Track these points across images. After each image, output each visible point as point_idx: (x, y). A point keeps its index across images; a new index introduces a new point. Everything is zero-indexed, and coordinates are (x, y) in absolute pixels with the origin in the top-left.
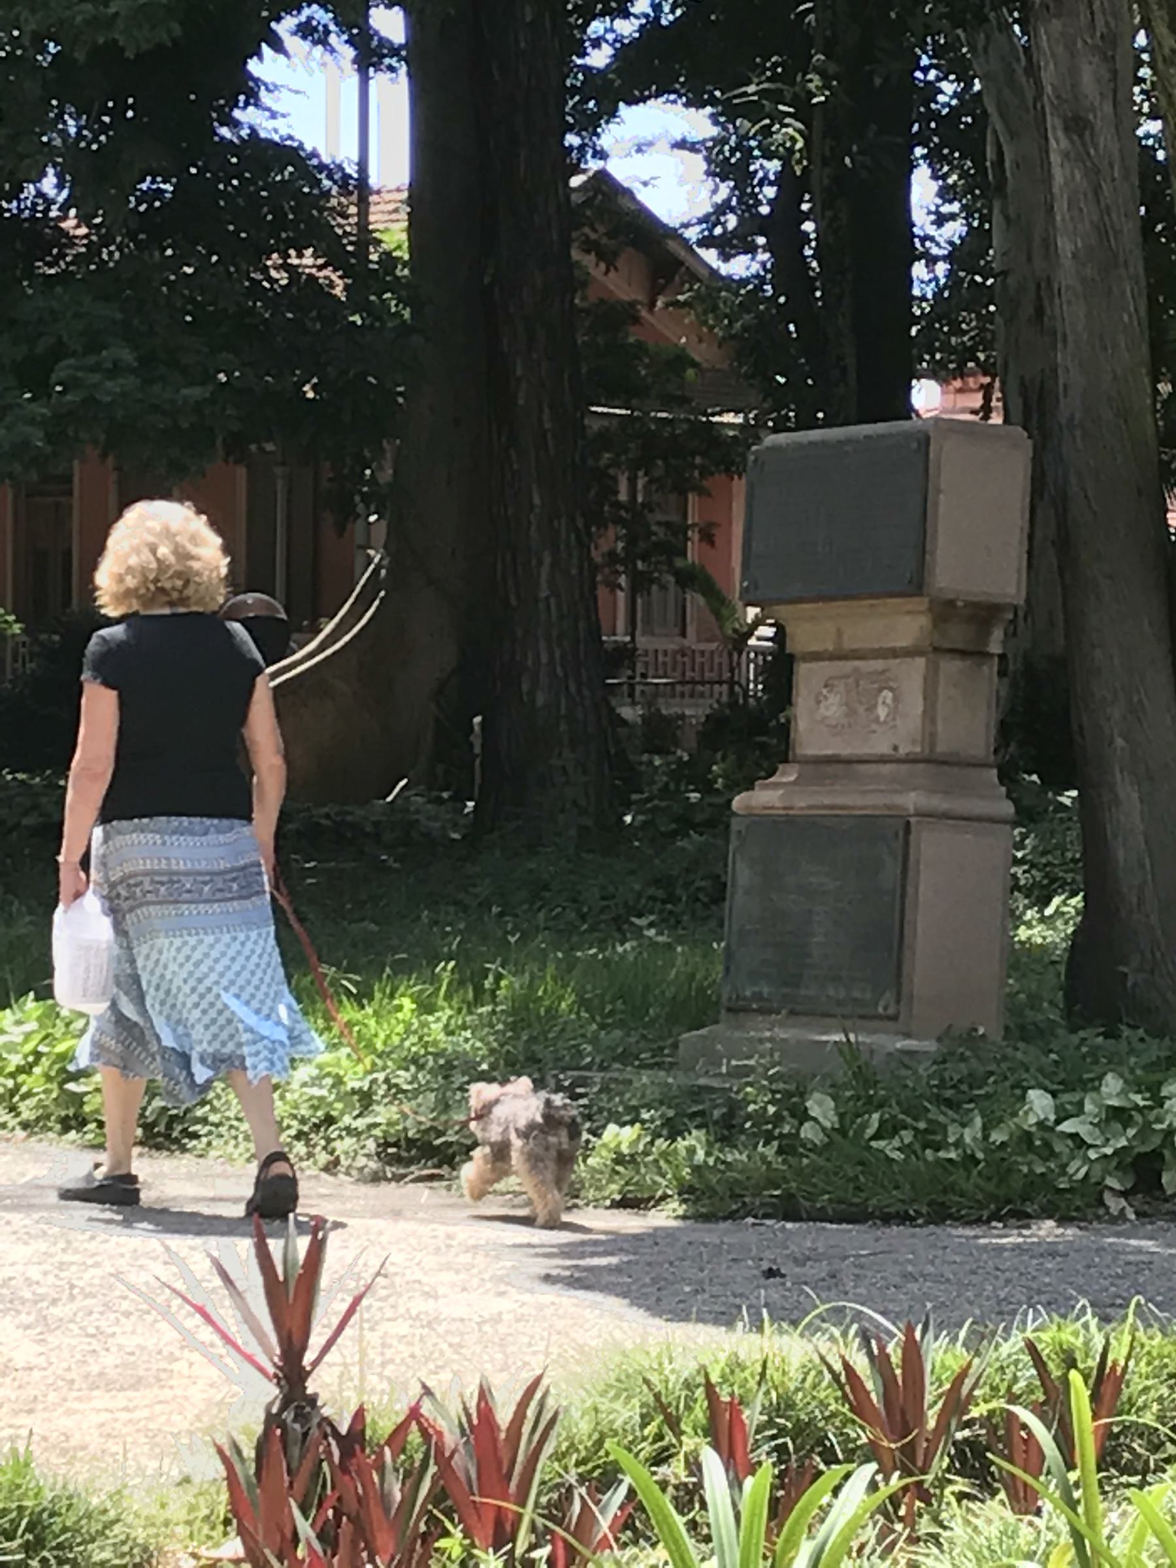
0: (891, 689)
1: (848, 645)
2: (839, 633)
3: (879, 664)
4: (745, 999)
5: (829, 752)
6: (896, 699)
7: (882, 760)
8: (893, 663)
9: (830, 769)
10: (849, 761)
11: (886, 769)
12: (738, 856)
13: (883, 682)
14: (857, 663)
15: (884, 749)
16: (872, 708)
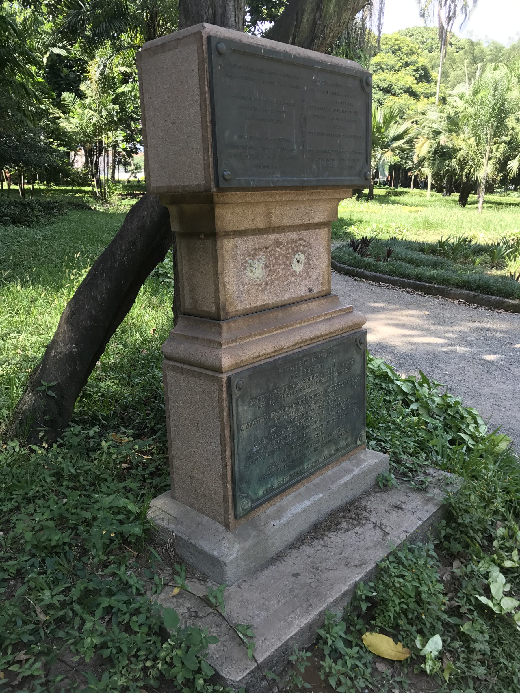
0: (303, 252)
1: (276, 221)
2: (269, 215)
3: (294, 236)
4: (258, 499)
5: (259, 304)
6: (307, 258)
7: (302, 301)
8: (305, 234)
9: (272, 315)
10: (284, 306)
11: (314, 305)
12: (240, 403)
13: (294, 248)
14: (278, 236)
15: (303, 292)
16: (288, 266)
